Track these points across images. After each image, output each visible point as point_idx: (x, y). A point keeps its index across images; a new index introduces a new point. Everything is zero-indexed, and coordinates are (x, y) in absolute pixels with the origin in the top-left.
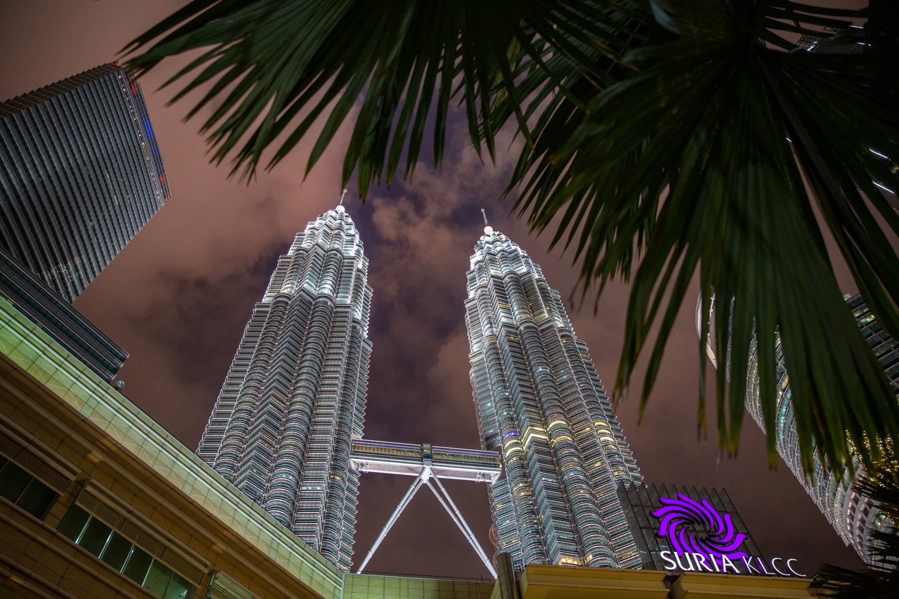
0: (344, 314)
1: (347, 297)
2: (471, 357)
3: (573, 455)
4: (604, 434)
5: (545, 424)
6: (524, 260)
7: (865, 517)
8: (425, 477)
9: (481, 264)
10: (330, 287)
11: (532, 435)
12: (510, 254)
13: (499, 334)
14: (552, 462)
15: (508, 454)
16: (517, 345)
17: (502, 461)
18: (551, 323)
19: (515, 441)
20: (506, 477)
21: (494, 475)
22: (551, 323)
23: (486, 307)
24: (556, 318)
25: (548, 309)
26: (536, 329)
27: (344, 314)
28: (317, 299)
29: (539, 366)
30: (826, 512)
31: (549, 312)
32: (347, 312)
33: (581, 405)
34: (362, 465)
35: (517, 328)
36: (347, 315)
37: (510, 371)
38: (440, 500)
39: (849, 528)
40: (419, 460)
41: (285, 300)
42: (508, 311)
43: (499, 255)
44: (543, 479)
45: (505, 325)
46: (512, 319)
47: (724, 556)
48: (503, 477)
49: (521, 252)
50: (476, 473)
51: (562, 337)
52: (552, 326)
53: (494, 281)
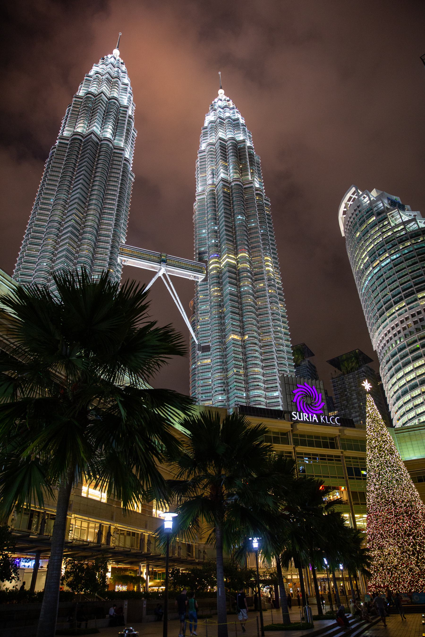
0: (120, 155)
1: (121, 141)
2: (197, 195)
3: (249, 277)
4: (268, 266)
5: (236, 254)
6: (242, 127)
7: (386, 343)
8: (160, 274)
9: (213, 124)
10: (110, 131)
11: (227, 260)
12: (234, 121)
13: (218, 184)
14: (235, 279)
15: (210, 268)
16: (227, 196)
17: (207, 270)
18: (252, 185)
19: (217, 260)
20: (207, 280)
21: (201, 277)
22: (252, 185)
23: (212, 161)
24: (256, 177)
25: (252, 171)
26: (242, 187)
27: (120, 155)
28: (102, 140)
29: (239, 214)
30: (371, 334)
31: (252, 173)
32: (122, 154)
33: (259, 247)
34: (125, 261)
35: (230, 183)
36: (122, 156)
37: (221, 213)
38: (168, 288)
39: (378, 345)
40: (158, 263)
41: (80, 138)
42: (226, 168)
43: (226, 121)
44: (229, 288)
45: (223, 180)
46: (227, 175)
47: (314, 415)
48: (205, 280)
49: (242, 121)
50: (191, 275)
51: (257, 194)
52: (252, 187)
53: (220, 142)
